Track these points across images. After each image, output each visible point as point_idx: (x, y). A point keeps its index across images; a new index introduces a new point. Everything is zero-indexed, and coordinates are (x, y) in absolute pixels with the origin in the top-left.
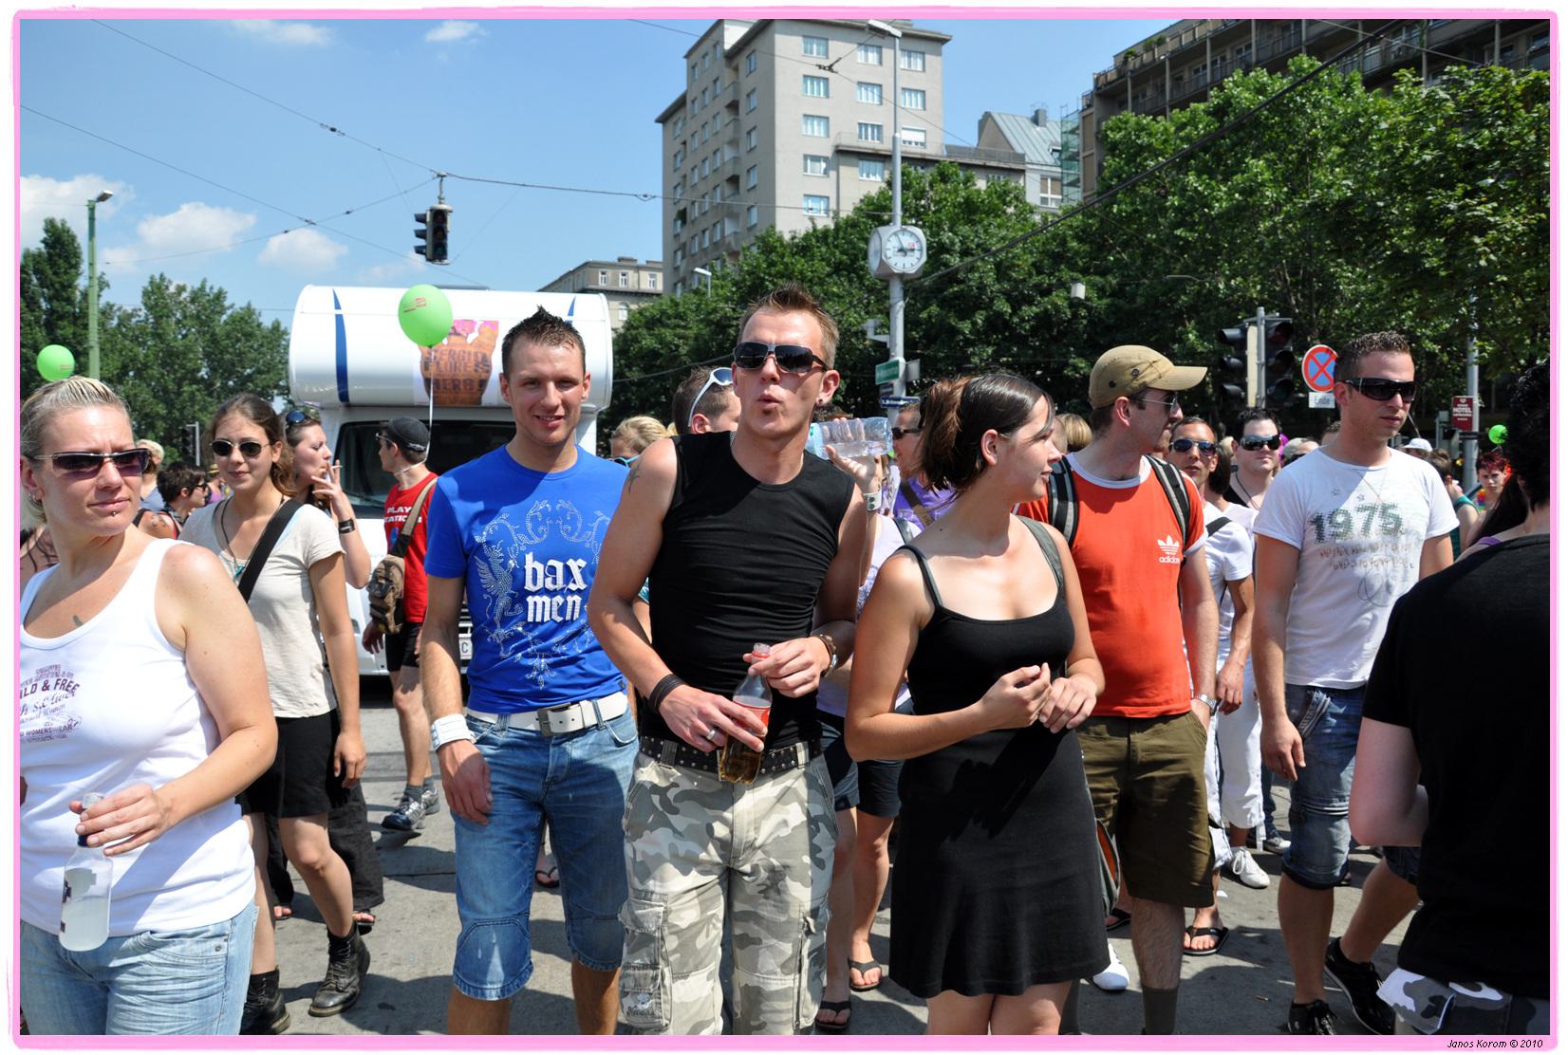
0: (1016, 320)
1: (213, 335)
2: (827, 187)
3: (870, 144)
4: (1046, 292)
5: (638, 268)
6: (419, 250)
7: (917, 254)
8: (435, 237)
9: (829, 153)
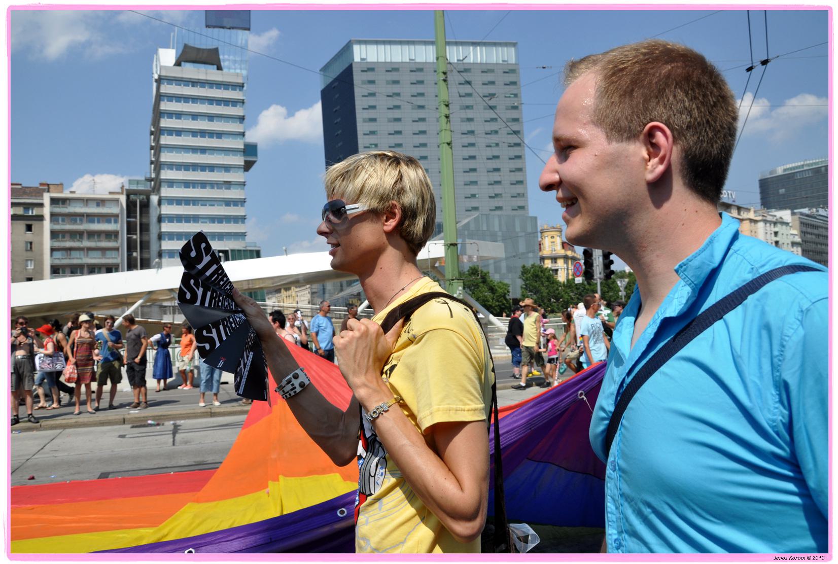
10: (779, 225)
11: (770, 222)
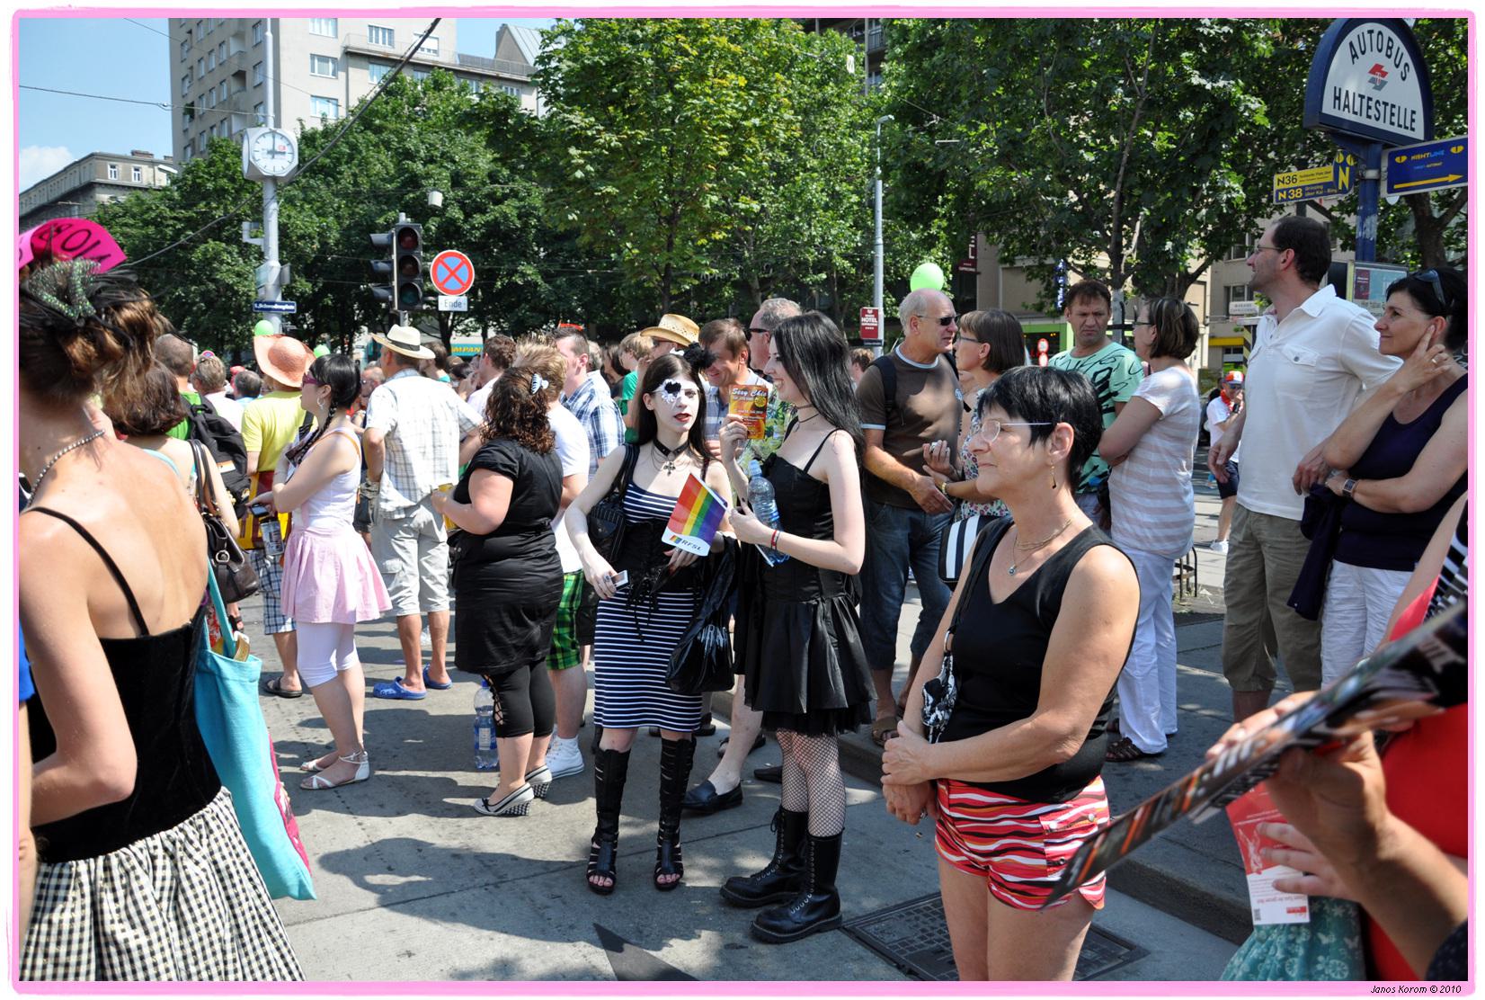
0: (467, 227)
4: (498, 202)
5: (153, 163)
7: (289, 157)
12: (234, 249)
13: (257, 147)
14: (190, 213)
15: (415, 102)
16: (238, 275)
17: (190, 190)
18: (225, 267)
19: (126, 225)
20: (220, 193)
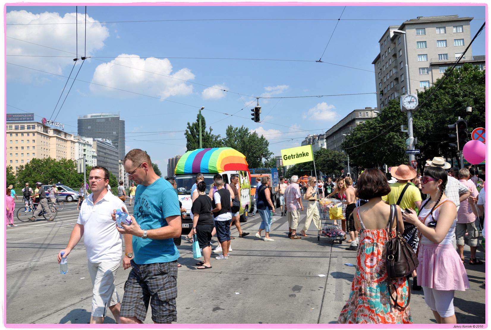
1: (244, 141)
2: (428, 77)
3: (443, 61)
5: (371, 110)
6: (253, 119)
7: (415, 103)
8: (256, 115)
9: (428, 66)
10: (86, 146)
11: (82, 144)
12: (398, 134)
13: (405, 101)
14: (385, 124)
15: (458, 76)
16: (400, 142)
17: (384, 117)
18: (395, 140)
19: (365, 130)
20: (393, 117)
